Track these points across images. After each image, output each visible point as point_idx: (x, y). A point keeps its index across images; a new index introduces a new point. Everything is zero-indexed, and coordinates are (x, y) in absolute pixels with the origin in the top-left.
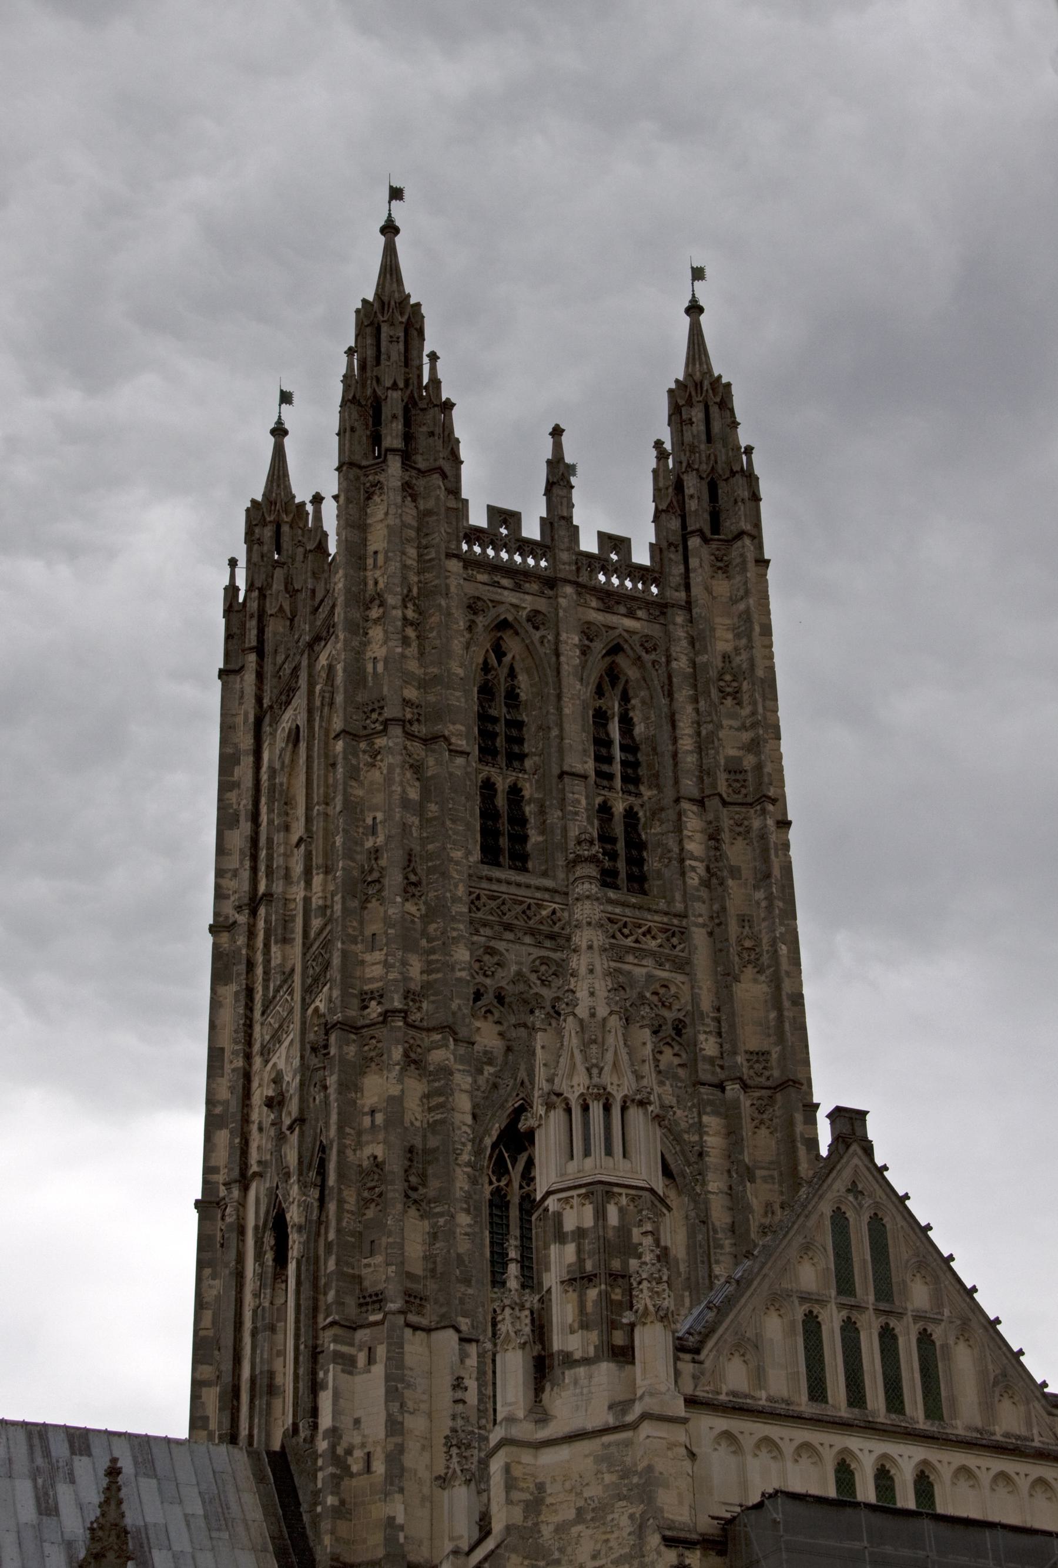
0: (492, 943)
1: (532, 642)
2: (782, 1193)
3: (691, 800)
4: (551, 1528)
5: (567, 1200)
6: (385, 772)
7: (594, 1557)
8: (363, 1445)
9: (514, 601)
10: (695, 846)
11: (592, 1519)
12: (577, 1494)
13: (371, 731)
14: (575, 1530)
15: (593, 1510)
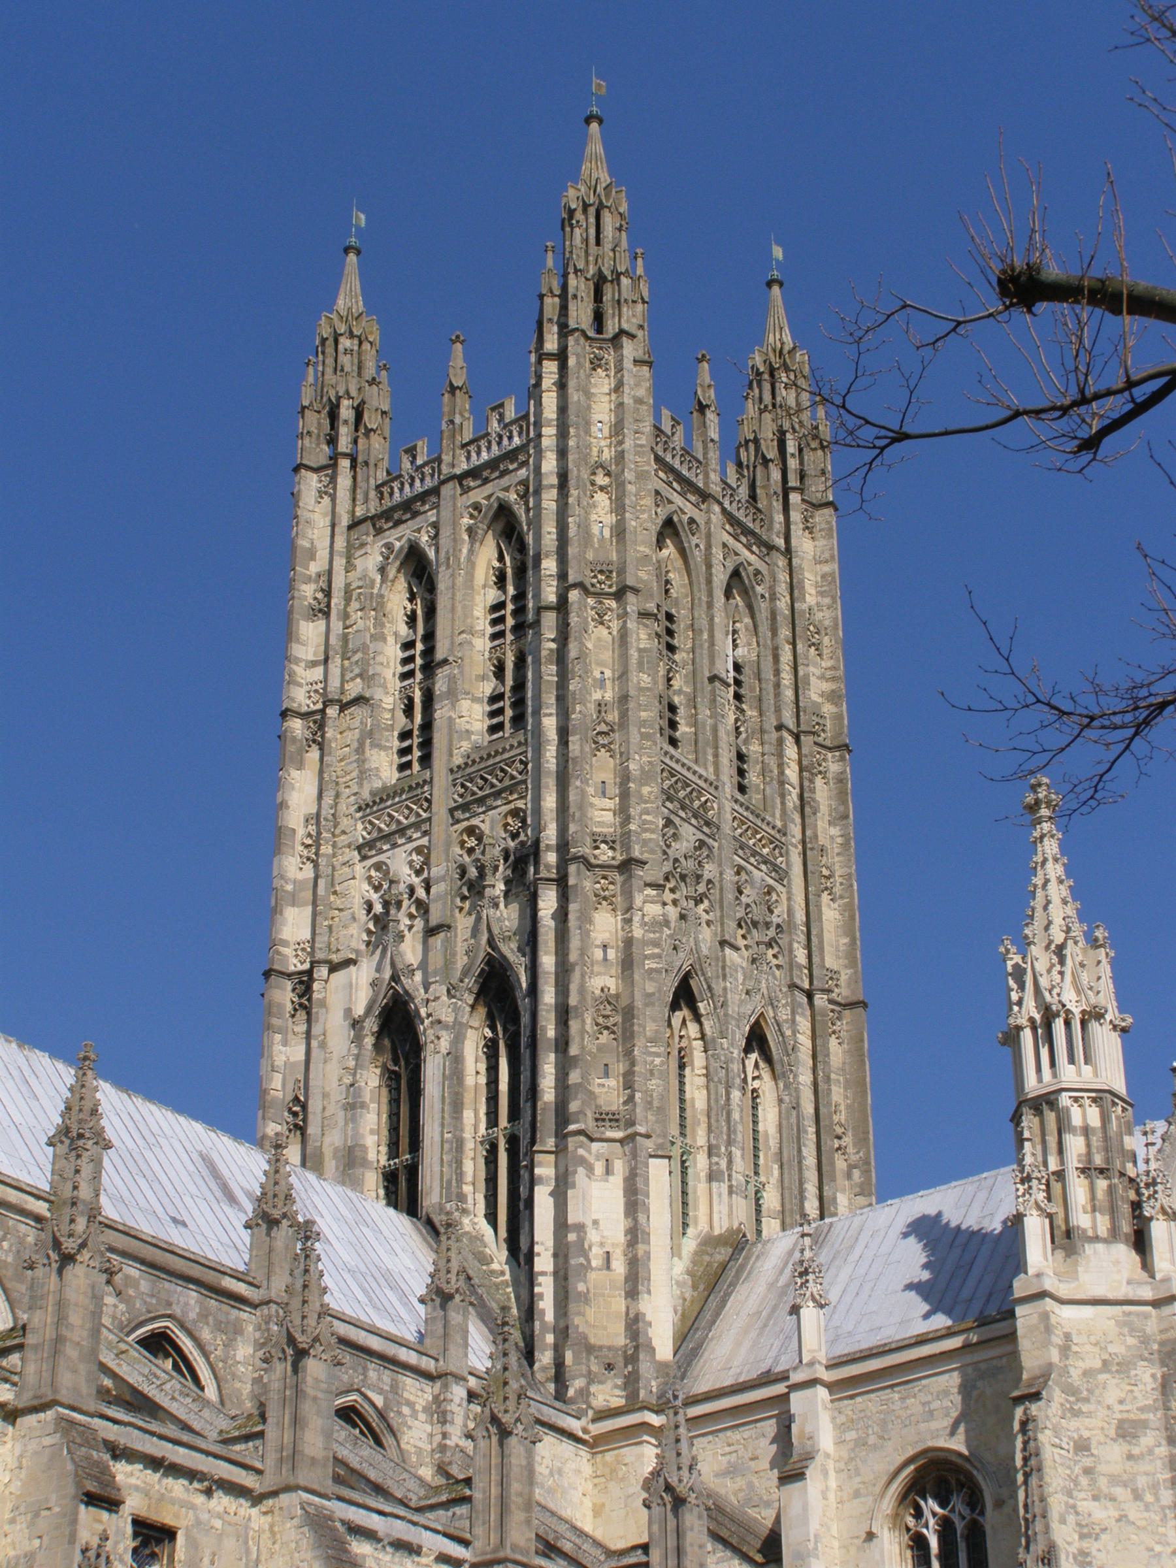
0: (673, 817)
1: (690, 547)
2: (846, 1097)
3: (789, 730)
4: (1080, 1372)
5: (1076, 1100)
6: (615, 633)
7: (1121, 1402)
8: (602, 1244)
9: (680, 504)
10: (792, 773)
11: (1117, 1371)
12: (1101, 1348)
13: (598, 590)
14: (1102, 1377)
15: (1118, 1364)
